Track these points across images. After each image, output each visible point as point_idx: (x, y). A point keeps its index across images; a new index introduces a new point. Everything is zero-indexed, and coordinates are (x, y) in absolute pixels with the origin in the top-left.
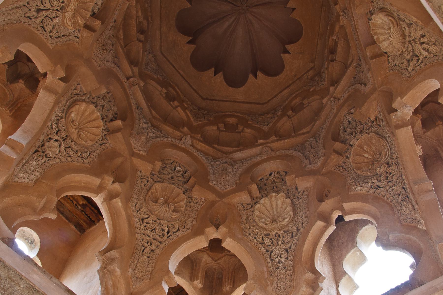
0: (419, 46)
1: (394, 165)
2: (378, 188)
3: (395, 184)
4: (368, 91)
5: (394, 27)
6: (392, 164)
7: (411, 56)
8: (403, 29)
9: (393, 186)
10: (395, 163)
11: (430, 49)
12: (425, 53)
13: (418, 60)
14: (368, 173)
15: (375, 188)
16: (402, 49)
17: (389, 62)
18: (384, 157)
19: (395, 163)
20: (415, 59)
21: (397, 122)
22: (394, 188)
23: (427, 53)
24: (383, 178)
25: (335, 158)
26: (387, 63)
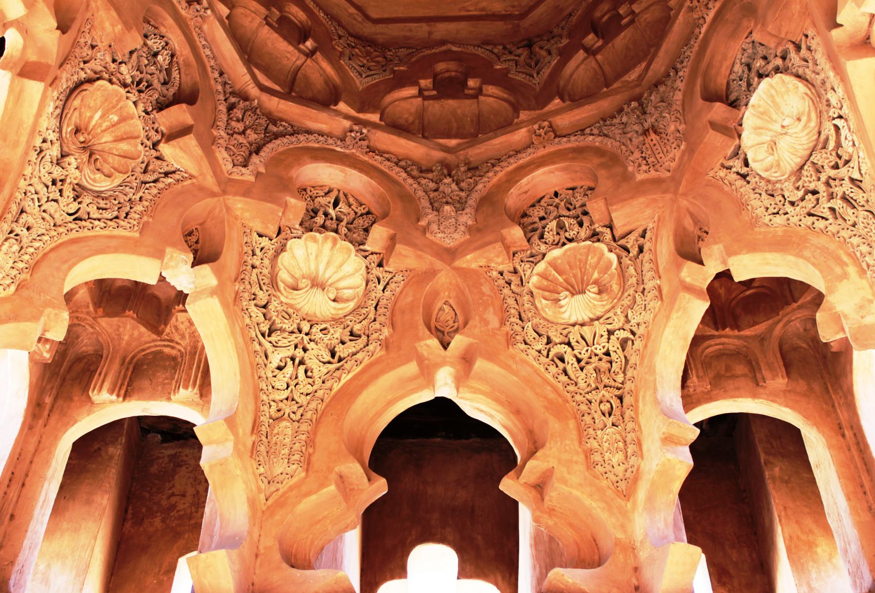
0: (291, 352)
1: (74, 207)
2: (39, 160)
3: (43, 208)
4: (218, 154)
5: (335, 308)
6: (79, 203)
7: (274, 321)
8: (323, 326)
9: (39, 201)
10: (79, 209)
11: (280, 375)
12: (275, 359)
13: (263, 335)
14: (69, 129)
15: (41, 151)
16: (287, 297)
17: (260, 236)
18: (92, 177)
19: (79, 209)
20: (265, 328)
21: (169, 256)
22: (37, 204)
23: (275, 364)
24: (55, 172)
25: (113, 29)
26: (261, 231)
